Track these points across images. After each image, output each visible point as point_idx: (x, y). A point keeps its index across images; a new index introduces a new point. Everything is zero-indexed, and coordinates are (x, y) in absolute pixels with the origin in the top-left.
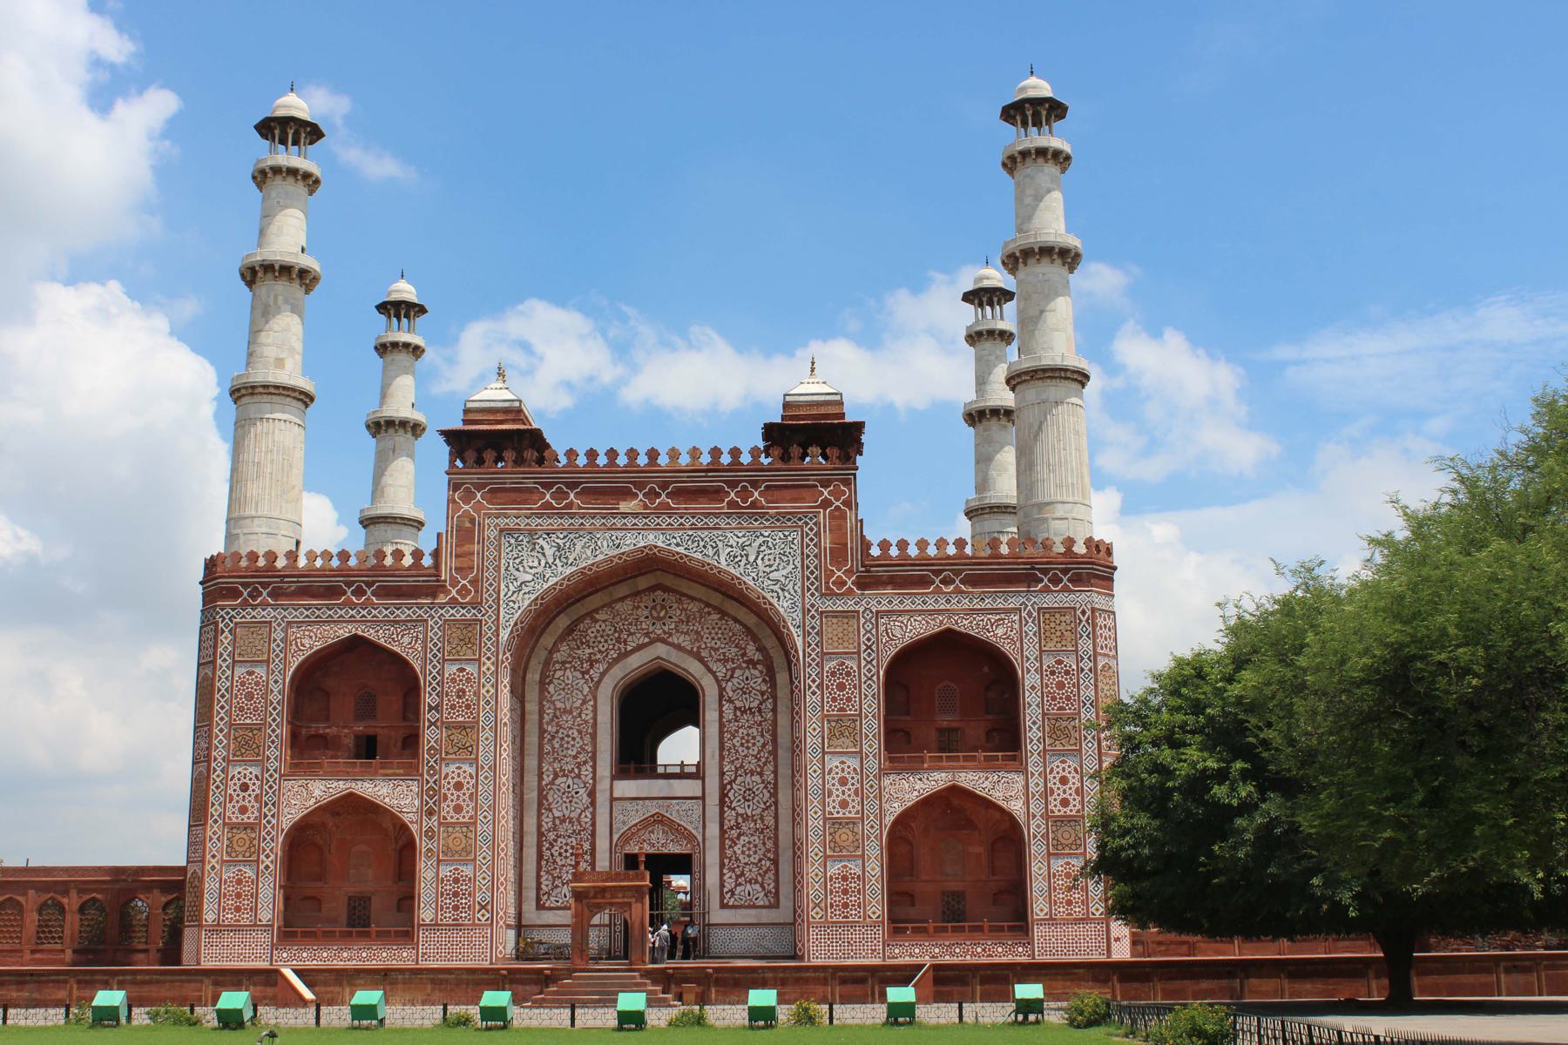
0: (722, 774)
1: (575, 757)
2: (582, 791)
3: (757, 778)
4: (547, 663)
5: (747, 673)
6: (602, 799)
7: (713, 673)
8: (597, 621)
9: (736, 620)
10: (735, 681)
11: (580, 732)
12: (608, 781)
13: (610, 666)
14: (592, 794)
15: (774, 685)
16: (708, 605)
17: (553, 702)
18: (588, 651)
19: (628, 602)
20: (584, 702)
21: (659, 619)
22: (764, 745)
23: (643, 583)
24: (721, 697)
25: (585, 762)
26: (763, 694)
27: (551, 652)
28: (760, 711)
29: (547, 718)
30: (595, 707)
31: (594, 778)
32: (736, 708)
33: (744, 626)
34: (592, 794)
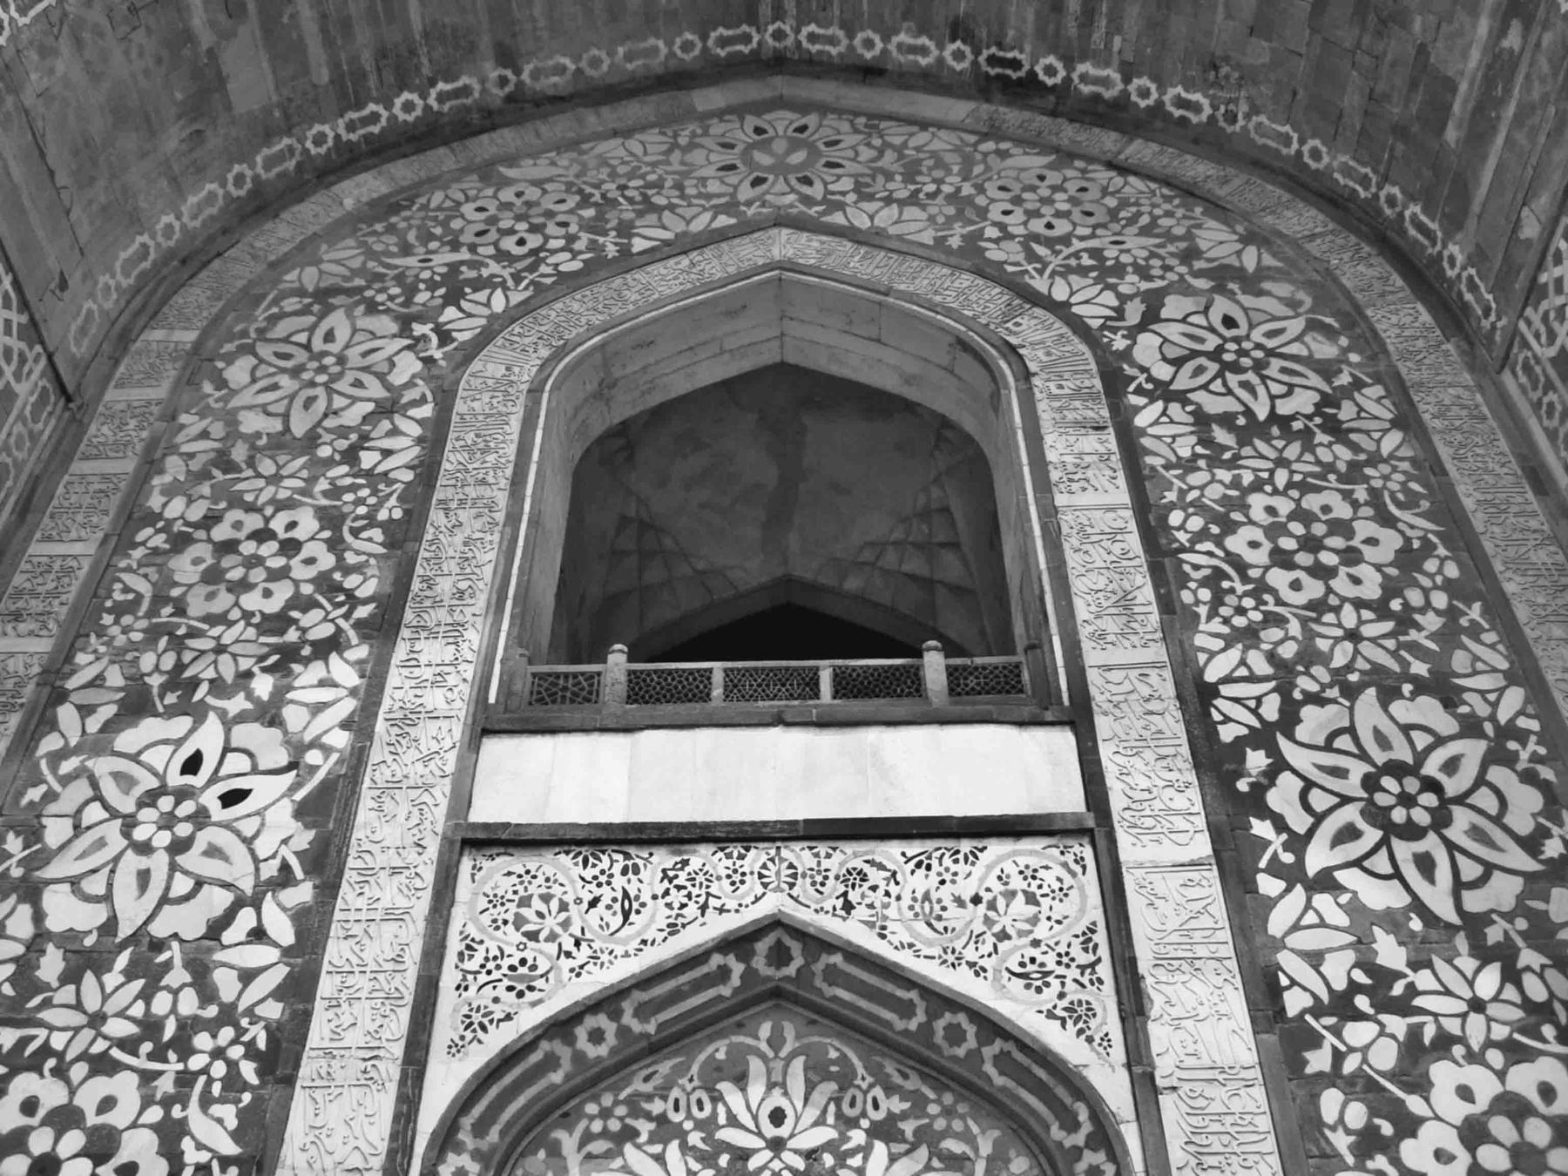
0: (1197, 697)
1: (277, 623)
2: (265, 789)
3: (1427, 710)
4: (250, 298)
5: (1221, 306)
6: (393, 834)
7: (1061, 310)
8: (508, 182)
9: (1124, 170)
10: (1173, 331)
11: (331, 519)
12: (445, 736)
13: (542, 296)
14: (329, 809)
15: (1370, 342)
16: (993, 132)
17: (231, 419)
18: (443, 258)
19: (652, 136)
20: (388, 408)
21: (781, 169)
22: (1409, 559)
23: (709, 98)
24: (1114, 382)
25: (331, 646)
26: (1327, 370)
27: (279, 266)
28: (1336, 429)
29: (174, 468)
30: (435, 438)
31: (360, 725)
32: (1202, 420)
33: (1167, 182)
34: (329, 809)
